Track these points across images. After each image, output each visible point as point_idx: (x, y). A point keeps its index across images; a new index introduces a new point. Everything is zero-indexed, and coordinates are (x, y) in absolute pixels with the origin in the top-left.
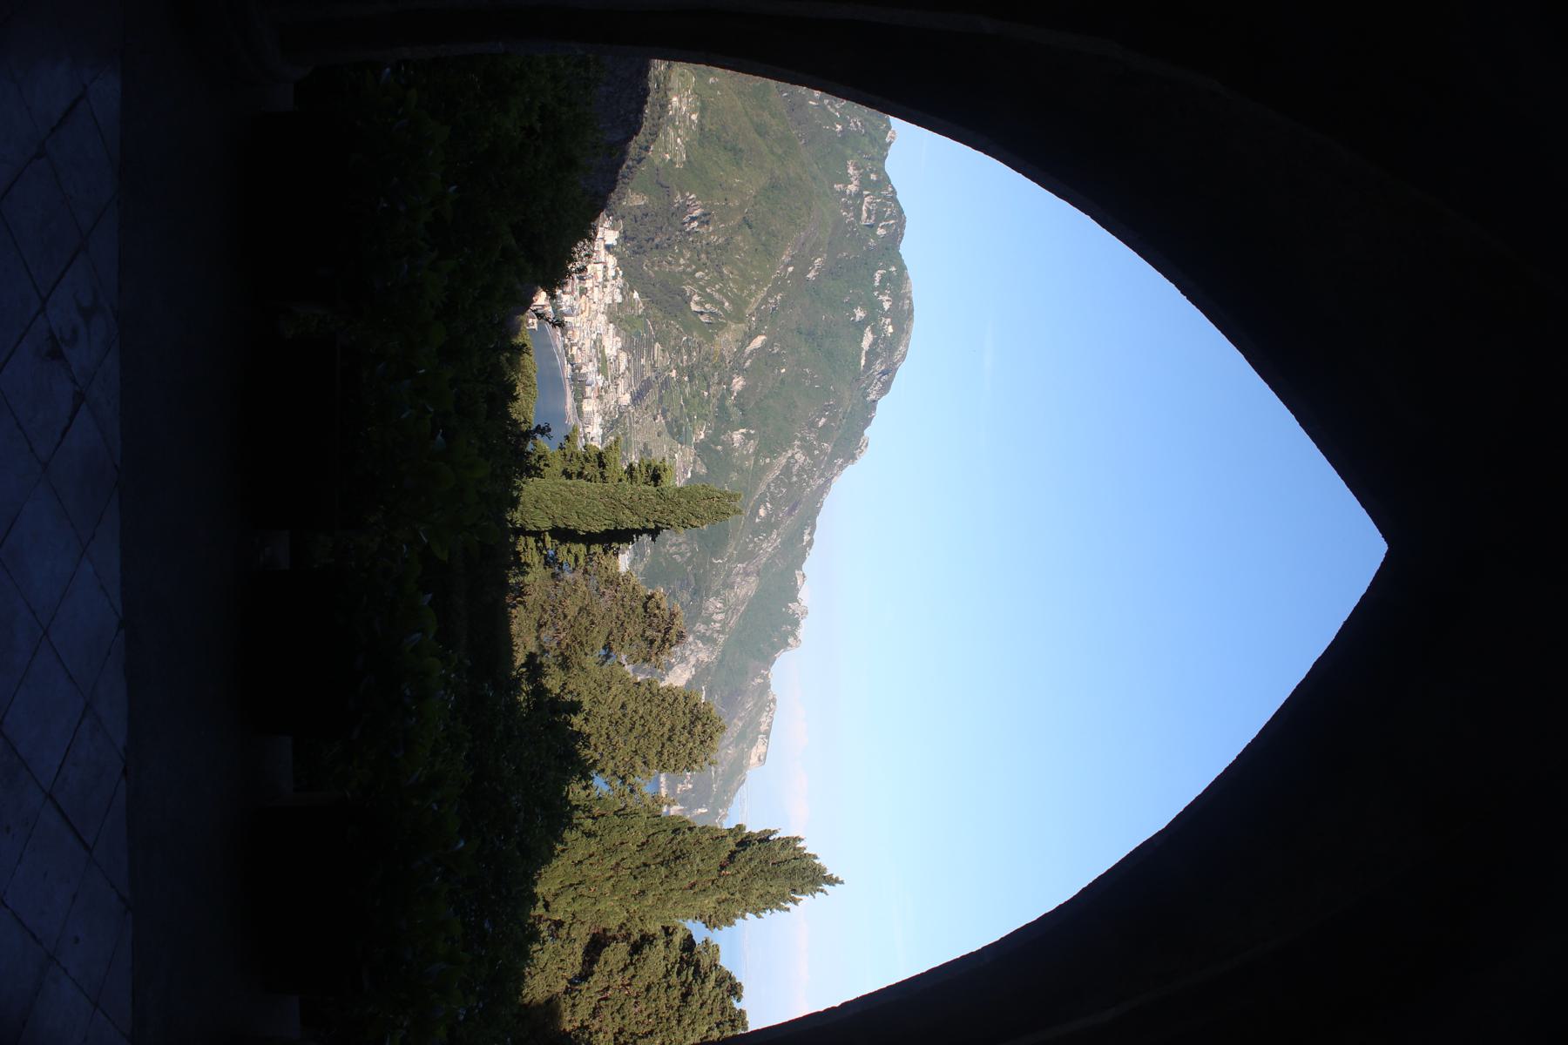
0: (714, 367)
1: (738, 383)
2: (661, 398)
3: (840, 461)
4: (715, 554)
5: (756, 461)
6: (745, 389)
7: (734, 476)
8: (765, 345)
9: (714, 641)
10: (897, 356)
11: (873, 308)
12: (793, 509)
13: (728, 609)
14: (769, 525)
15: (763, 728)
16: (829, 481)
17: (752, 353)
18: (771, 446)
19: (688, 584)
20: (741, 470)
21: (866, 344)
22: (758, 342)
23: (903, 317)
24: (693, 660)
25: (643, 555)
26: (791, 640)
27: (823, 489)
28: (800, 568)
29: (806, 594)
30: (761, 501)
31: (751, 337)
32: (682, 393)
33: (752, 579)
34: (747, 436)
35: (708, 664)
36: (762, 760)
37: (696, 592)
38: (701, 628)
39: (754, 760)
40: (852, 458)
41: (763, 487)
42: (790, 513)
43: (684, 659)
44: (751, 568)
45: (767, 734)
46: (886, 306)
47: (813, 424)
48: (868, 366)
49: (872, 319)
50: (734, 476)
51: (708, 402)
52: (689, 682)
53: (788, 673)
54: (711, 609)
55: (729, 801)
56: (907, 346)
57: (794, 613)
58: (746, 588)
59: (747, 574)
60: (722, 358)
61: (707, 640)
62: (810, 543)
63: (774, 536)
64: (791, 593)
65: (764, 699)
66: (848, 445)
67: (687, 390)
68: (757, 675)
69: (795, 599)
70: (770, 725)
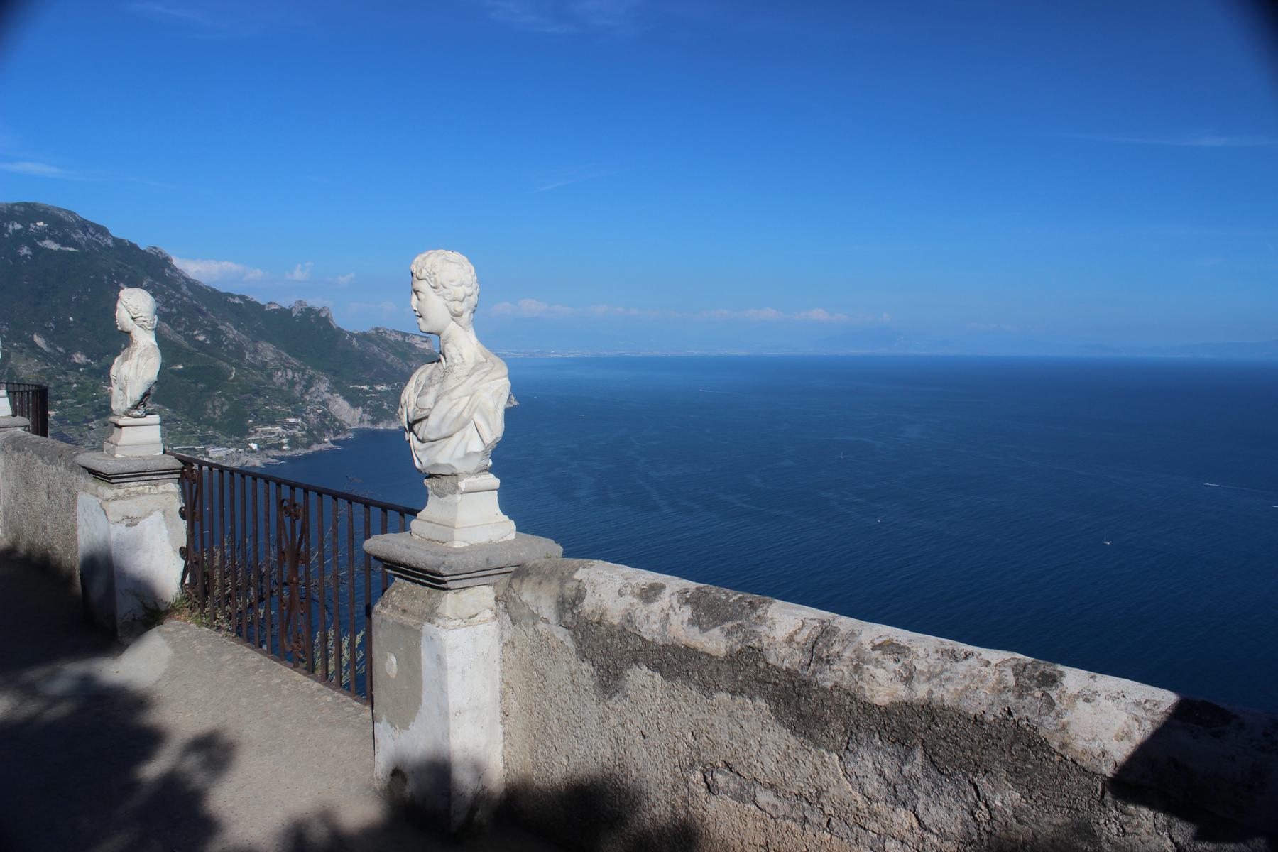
0: (50, 379)
1: (79, 358)
2: (74, 424)
3: (167, 272)
6: (84, 352)
8: (43, 334)
9: (311, 378)
11: (19, 238)
12: (201, 312)
13: (284, 366)
14: (214, 333)
15: (400, 338)
17: (51, 347)
19: (250, 399)
21: (54, 246)
22: (39, 340)
23: (30, 212)
24: (328, 395)
25: (213, 437)
26: (323, 315)
27: (193, 285)
28: (264, 306)
29: (256, 298)
30: (192, 339)
31: (34, 346)
32: (72, 405)
33: (260, 347)
35: (331, 382)
37: (257, 393)
38: (299, 388)
39: (426, 346)
40: (166, 262)
41: (180, 339)
44: (251, 347)
45: (405, 335)
46: (18, 227)
48: (75, 244)
49: (31, 239)
51: (82, 384)
52: (346, 398)
53: (351, 317)
54: (282, 380)
56: (60, 210)
58: (268, 351)
59: (256, 351)
60: (44, 371)
63: (223, 328)
64: (285, 313)
67: (70, 401)
68: (349, 343)
69: (289, 311)
70: (397, 332)
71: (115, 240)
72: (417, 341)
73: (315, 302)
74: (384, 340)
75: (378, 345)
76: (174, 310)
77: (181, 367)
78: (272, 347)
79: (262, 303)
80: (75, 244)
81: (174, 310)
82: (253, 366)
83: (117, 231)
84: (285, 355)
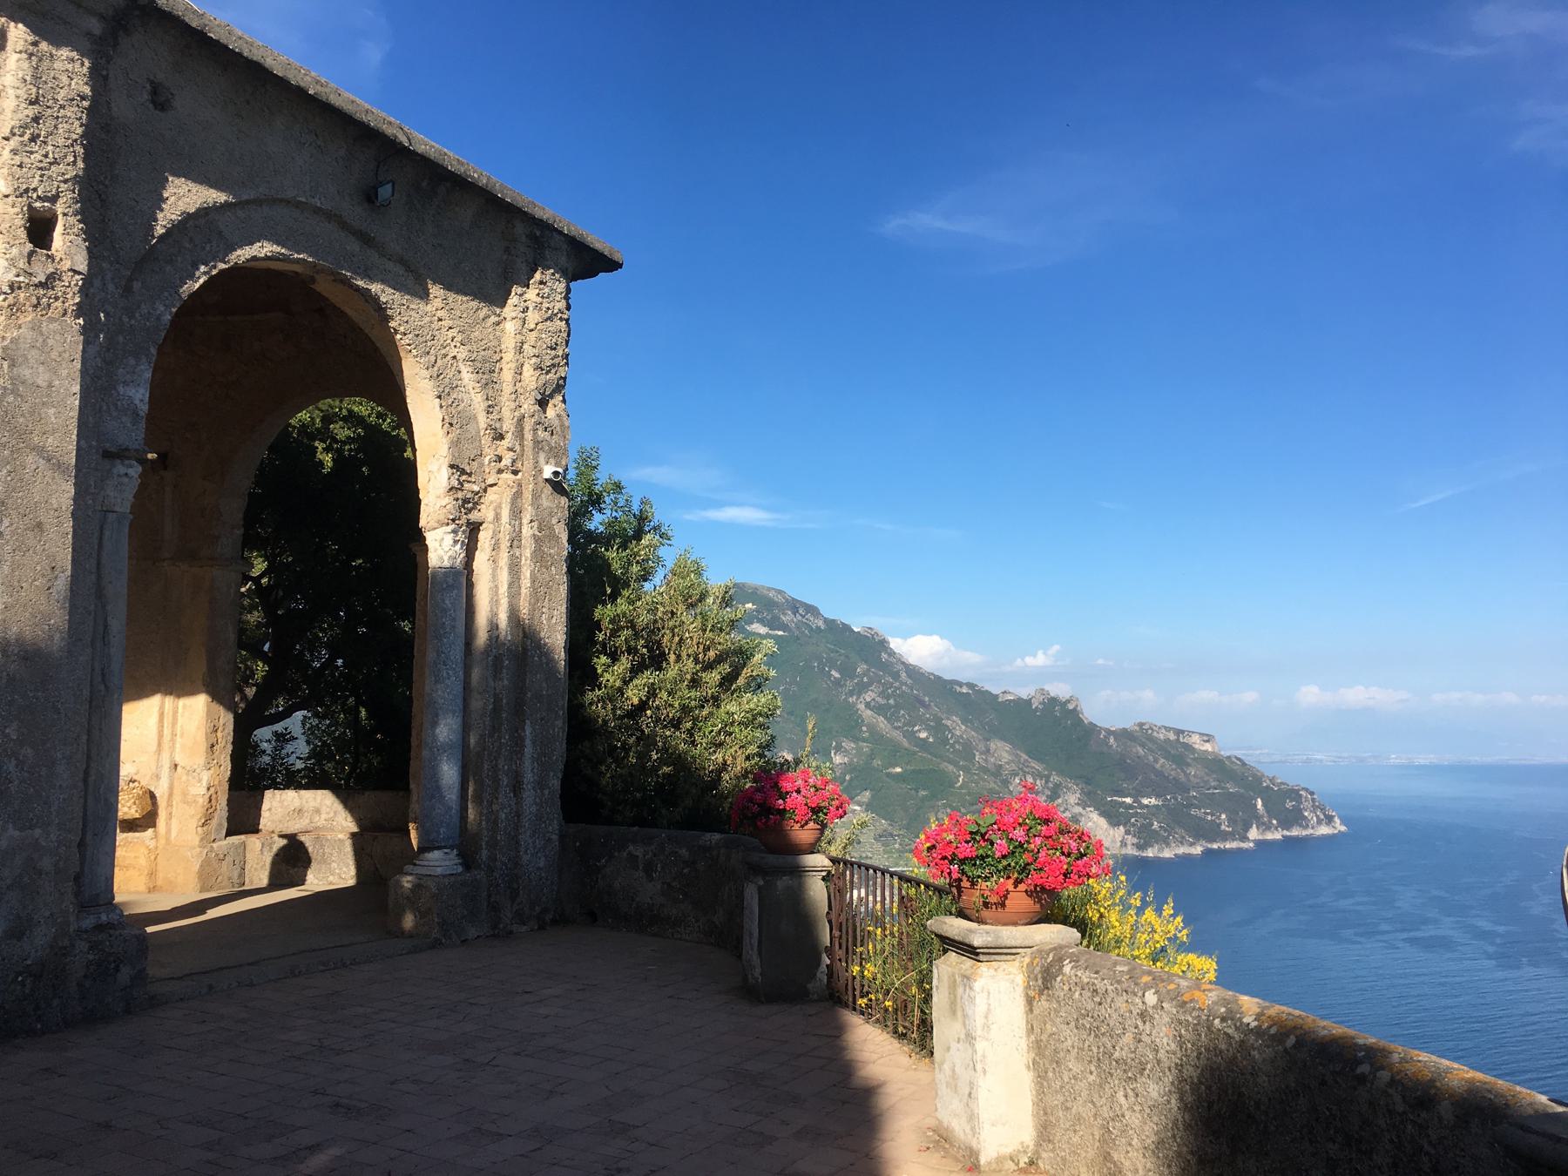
4: (952, 785)
5: (864, 740)
7: (877, 763)
9: (1057, 786)
10: (779, 599)
13: (1022, 770)
14: (938, 728)
15: (1172, 737)
16: (906, 666)
18: (851, 725)
20: (872, 756)
26: (1071, 707)
27: (913, 671)
30: (911, 736)
33: (993, 746)
34: (838, 749)
35: (1083, 792)
36: (1208, 738)
39: (1208, 747)
40: (883, 644)
42: (927, 707)
43: (1075, 819)
44: (982, 747)
45: (1179, 732)
47: (837, 683)
48: (784, 627)
50: (877, 763)
52: (1102, 814)
53: (1108, 707)
55: (1254, 776)
56: (769, 589)
57: (1043, 703)
58: (1002, 752)
59: (988, 750)
61: (1054, 795)
62: (971, 685)
63: (949, 723)
64: (1022, 705)
65: (1140, 736)
66: (872, 648)
68: (1105, 742)
69: (1029, 702)
70: (1168, 729)
71: (826, 620)
72: (1195, 741)
73: (1060, 690)
74: (1151, 739)
75: (1143, 746)
76: (891, 701)
77: (899, 770)
78: (1008, 747)
79: (995, 691)
80: (784, 627)
81: (891, 701)
82: (985, 770)
83: (831, 610)
84: (1024, 756)
